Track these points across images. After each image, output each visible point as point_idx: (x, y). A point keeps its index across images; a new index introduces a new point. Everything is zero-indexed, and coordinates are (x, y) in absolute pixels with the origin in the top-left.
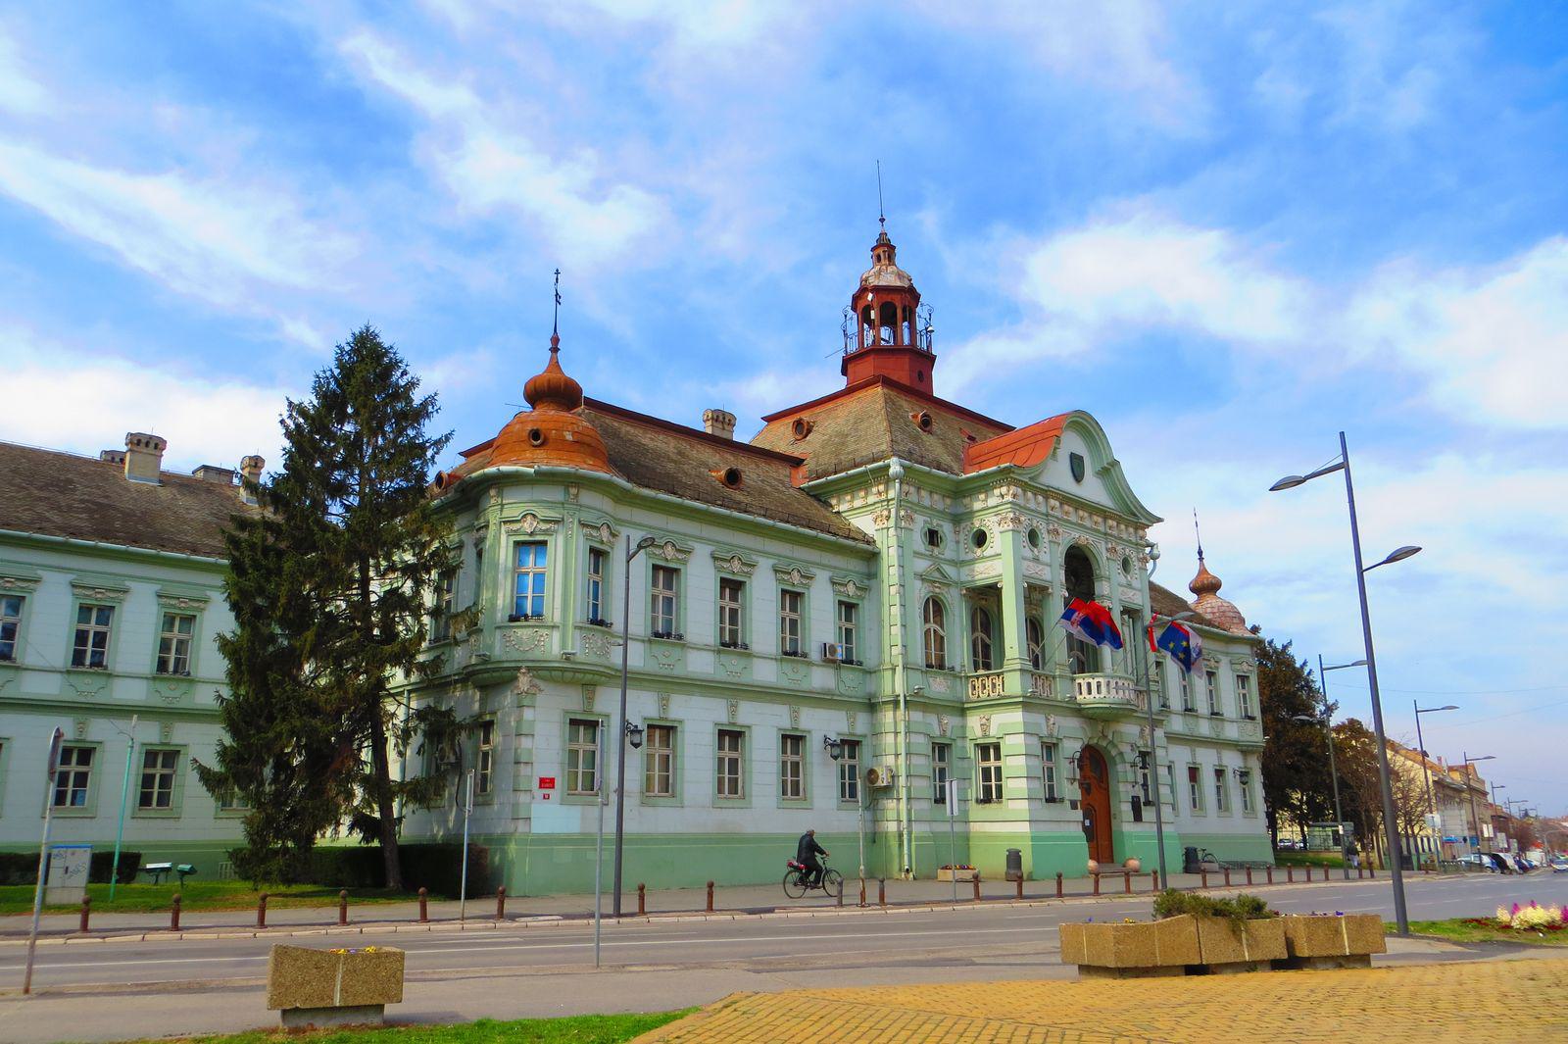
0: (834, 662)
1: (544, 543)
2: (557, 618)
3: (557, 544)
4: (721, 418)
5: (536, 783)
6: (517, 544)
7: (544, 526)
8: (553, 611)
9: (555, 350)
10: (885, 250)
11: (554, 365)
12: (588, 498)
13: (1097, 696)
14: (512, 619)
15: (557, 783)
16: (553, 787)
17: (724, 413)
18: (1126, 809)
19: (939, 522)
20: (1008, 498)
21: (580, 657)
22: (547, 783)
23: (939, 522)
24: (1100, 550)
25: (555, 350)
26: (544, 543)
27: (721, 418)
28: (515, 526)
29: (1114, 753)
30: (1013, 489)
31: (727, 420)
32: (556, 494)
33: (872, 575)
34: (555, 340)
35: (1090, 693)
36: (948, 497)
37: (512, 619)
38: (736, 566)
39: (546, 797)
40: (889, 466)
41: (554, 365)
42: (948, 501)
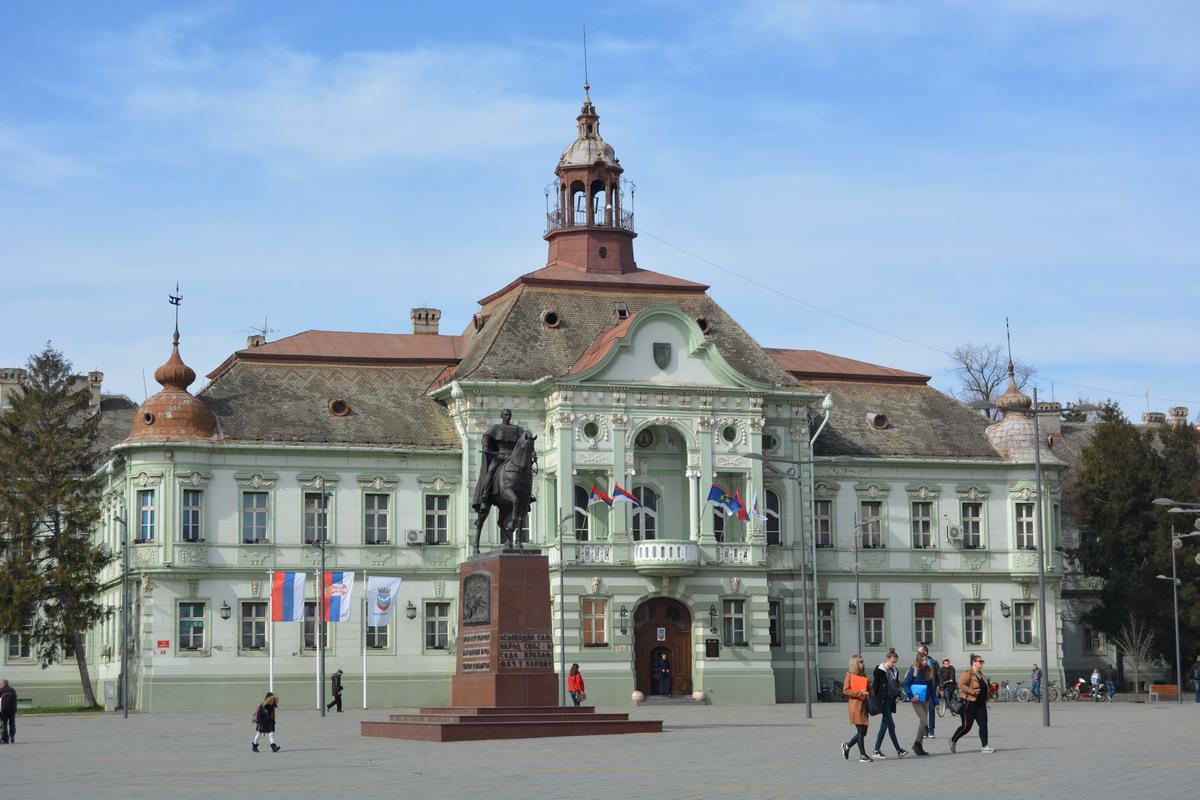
0: (419, 544)
1: (152, 491)
2: (162, 540)
3: (160, 491)
4: (423, 316)
5: (156, 644)
6: (139, 492)
7: (152, 480)
8: (159, 537)
9: (176, 344)
10: (589, 119)
11: (176, 357)
12: (180, 457)
13: (645, 559)
14: (137, 542)
15: (172, 644)
16: (168, 646)
17: (427, 311)
18: (699, 648)
19: (523, 421)
20: (560, 401)
21: (178, 563)
22: (163, 644)
23: (523, 421)
24: (691, 426)
25: (176, 344)
26: (152, 491)
27: (423, 316)
28: (136, 481)
29: (690, 603)
30: (563, 393)
31: (430, 316)
32: (160, 457)
33: (460, 471)
34: (177, 336)
35: (655, 556)
36: (533, 397)
37: (137, 542)
38: (318, 483)
39: (164, 653)
40: (451, 389)
41: (176, 357)
42: (533, 401)
